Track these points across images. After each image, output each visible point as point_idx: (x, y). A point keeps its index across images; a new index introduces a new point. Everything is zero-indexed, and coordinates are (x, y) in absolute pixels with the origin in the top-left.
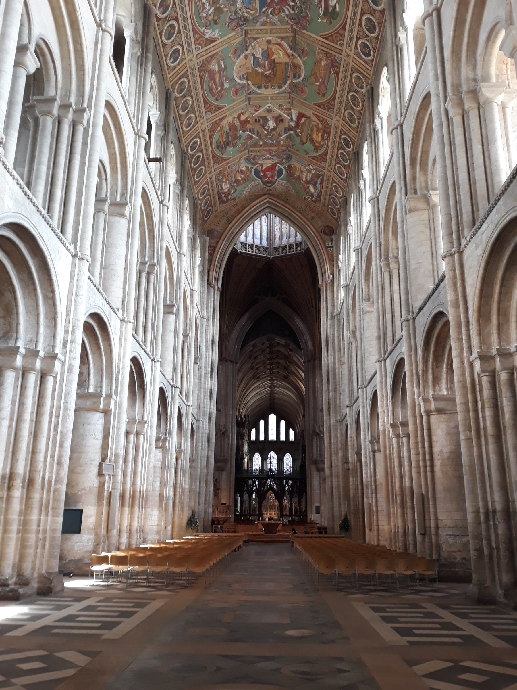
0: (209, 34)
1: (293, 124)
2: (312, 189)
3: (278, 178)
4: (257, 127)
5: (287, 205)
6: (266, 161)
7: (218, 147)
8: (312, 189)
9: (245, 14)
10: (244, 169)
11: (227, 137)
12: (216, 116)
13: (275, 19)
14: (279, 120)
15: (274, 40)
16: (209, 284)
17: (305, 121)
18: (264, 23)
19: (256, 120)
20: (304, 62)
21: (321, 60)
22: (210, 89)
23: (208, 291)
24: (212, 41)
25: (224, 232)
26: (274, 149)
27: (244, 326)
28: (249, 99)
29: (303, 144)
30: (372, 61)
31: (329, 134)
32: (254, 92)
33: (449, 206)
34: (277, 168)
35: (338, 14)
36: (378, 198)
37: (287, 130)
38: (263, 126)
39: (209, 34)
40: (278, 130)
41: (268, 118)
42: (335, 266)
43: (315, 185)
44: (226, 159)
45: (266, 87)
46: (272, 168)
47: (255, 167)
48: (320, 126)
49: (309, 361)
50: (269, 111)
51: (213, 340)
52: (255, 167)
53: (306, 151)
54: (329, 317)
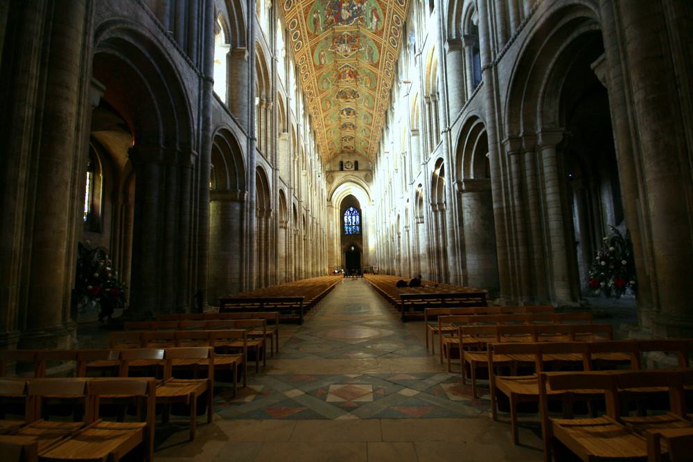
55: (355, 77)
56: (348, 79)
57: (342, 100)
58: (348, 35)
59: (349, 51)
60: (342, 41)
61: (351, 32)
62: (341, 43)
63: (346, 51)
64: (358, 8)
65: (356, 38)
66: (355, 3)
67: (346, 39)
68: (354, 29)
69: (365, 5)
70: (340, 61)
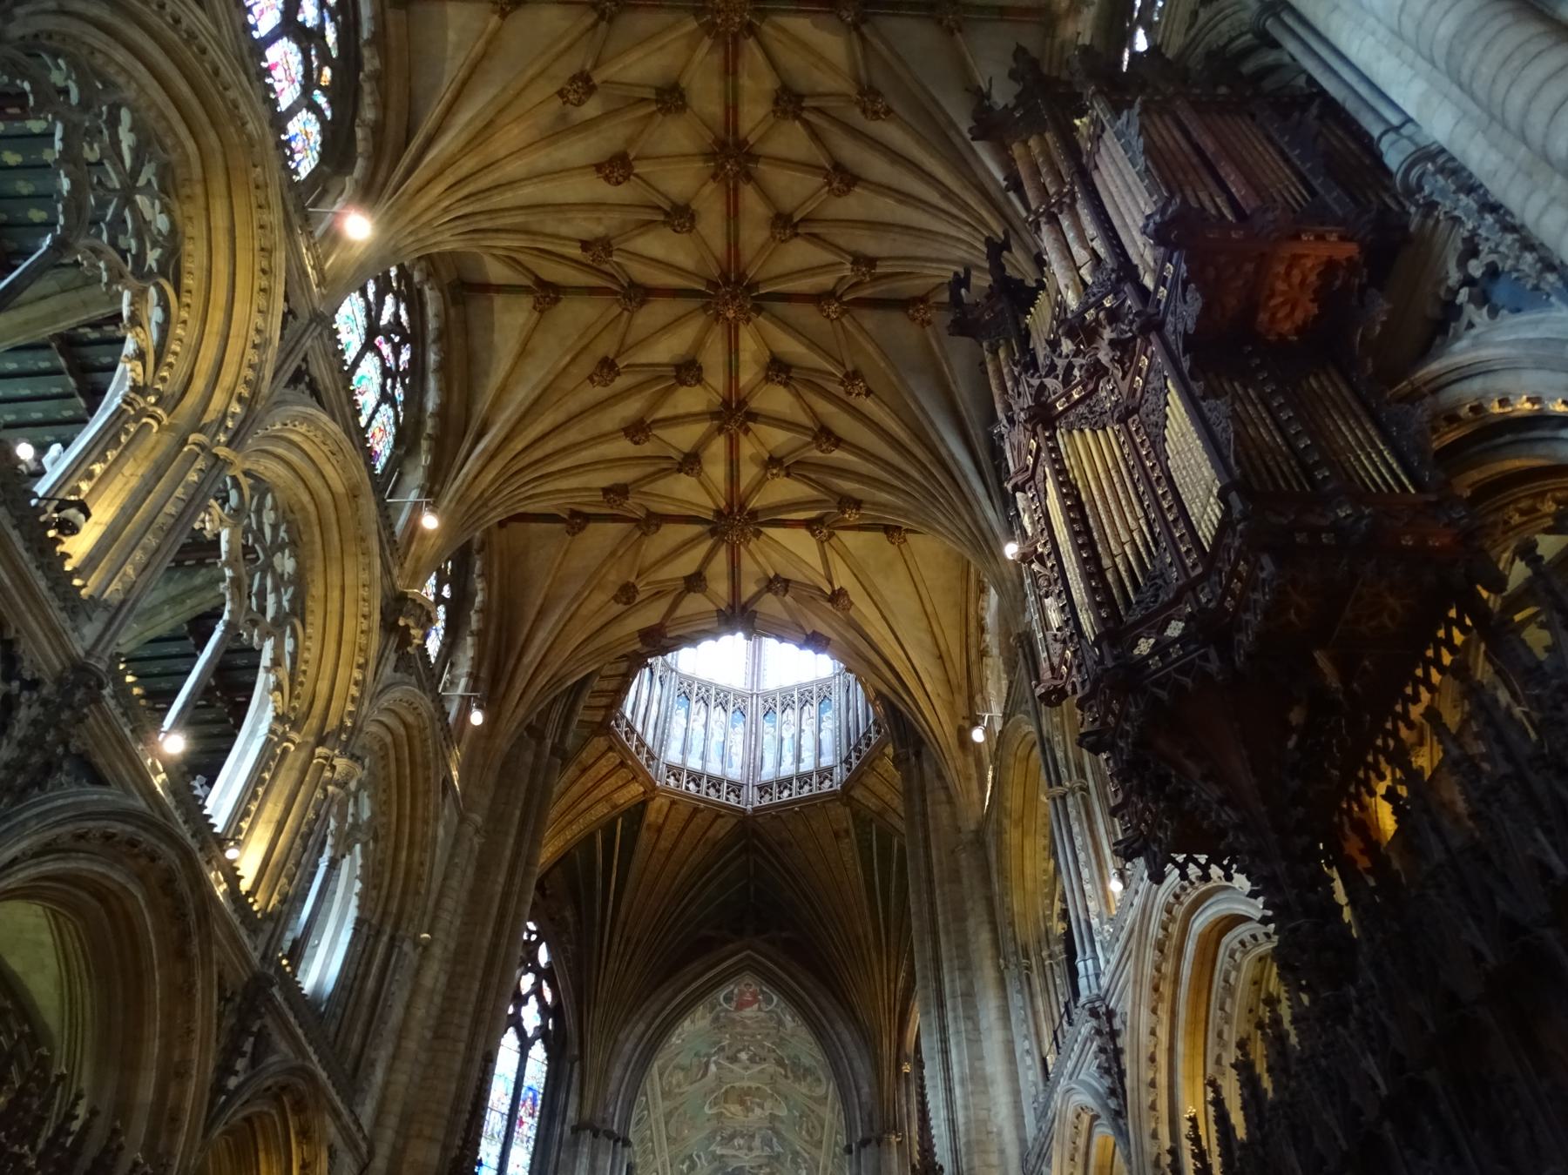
0: (806, 1155)
4: (764, 1053)
6: (753, 1015)
14: (734, 1059)
15: (742, 1118)
26: (739, 1029)
34: (734, 1004)
37: (722, 1049)
38: (755, 1054)
39: (806, 1155)
40: (734, 1049)
45: (750, 1088)
46: (741, 1006)
47: (770, 1008)
50: (747, 1068)
52: (770, 1008)
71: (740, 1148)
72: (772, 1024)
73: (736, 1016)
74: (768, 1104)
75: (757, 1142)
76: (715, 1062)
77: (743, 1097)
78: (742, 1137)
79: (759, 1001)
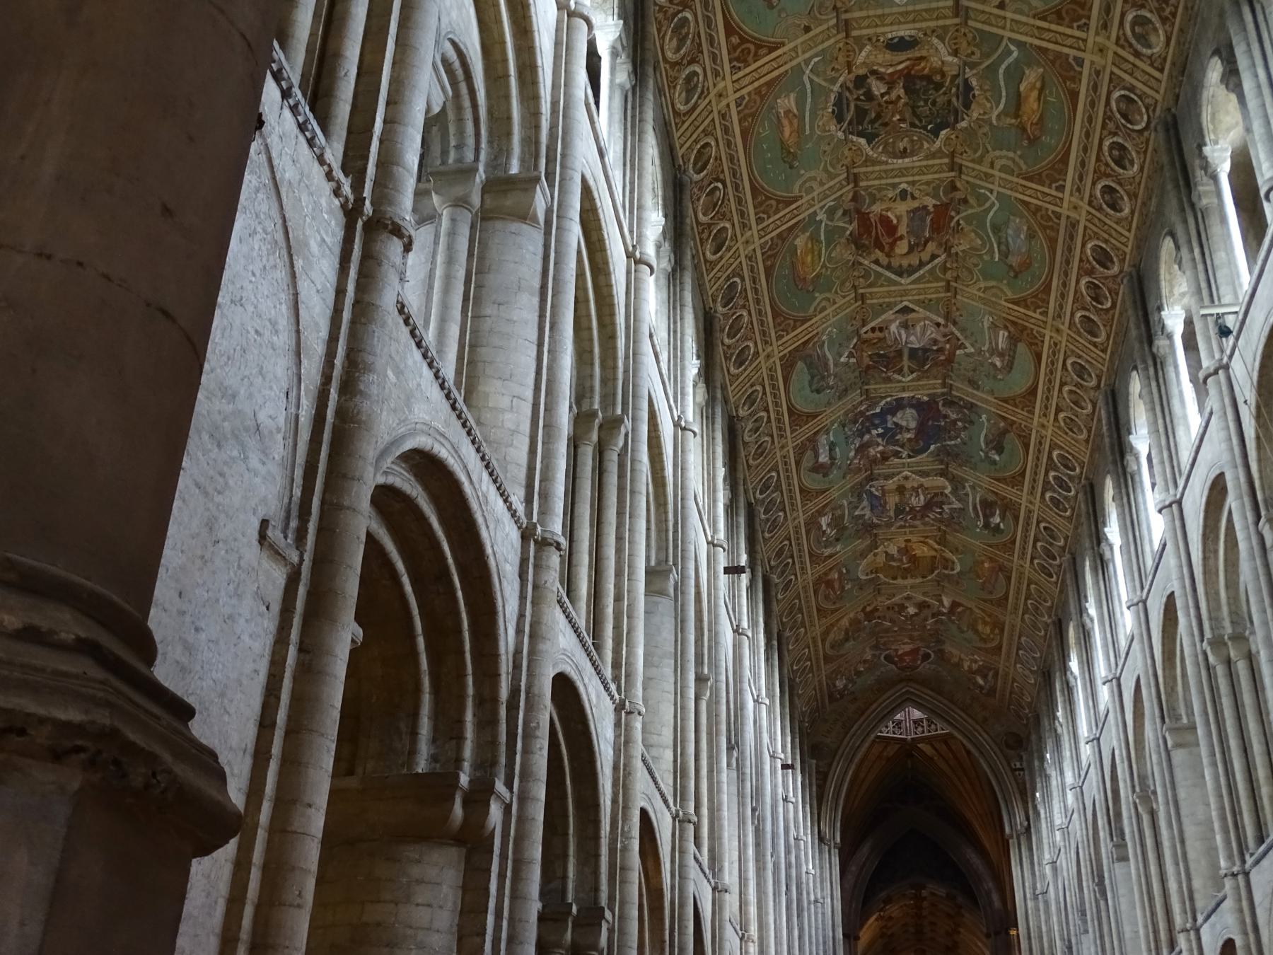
0: (827, 552)
1: (944, 610)
2: (981, 681)
3: (923, 661)
5: (940, 698)
7: (832, 647)
8: (981, 681)
9: (875, 521)
10: (869, 657)
11: (847, 631)
12: (831, 619)
13: (917, 523)
14: (922, 606)
15: (914, 538)
16: (821, 839)
17: (963, 611)
18: (901, 527)
19: (888, 608)
20: (958, 559)
21: (983, 562)
22: (827, 597)
23: (821, 852)
24: (830, 556)
25: (839, 748)
26: (916, 634)
27: (864, 864)
28: (879, 590)
29: (963, 632)
30: (1056, 583)
31: (1002, 630)
32: (885, 583)
33: (1145, 916)
34: (921, 653)
35: (1002, 531)
36: (1081, 787)
39: (827, 552)
40: (922, 615)
41: (907, 604)
42: (1030, 805)
43: (985, 677)
44: (842, 656)
45: (904, 578)
46: (915, 652)
48: (987, 619)
49: (997, 933)
50: (908, 598)
51: (834, 938)
53: (965, 639)
54: (1028, 895)
55: (864, 219)
56: (902, 208)
57: (941, 55)
58: (900, 371)
59: (893, 328)
60: (920, 357)
61: (889, 380)
62: (925, 350)
63: (905, 325)
64: (869, 432)
65: (868, 367)
66: (879, 440)
67: (906, 362)
68: (876, 387)
69: (852, 454)
70: (934, 290)
71: (915, 489)
72: (882, 641)
73: (919, 644)
74: (881, 559)
75: (892, 500)
76: (943, 606)
77: (914, 565)
78: (912, 509)
79: (897, 656)
